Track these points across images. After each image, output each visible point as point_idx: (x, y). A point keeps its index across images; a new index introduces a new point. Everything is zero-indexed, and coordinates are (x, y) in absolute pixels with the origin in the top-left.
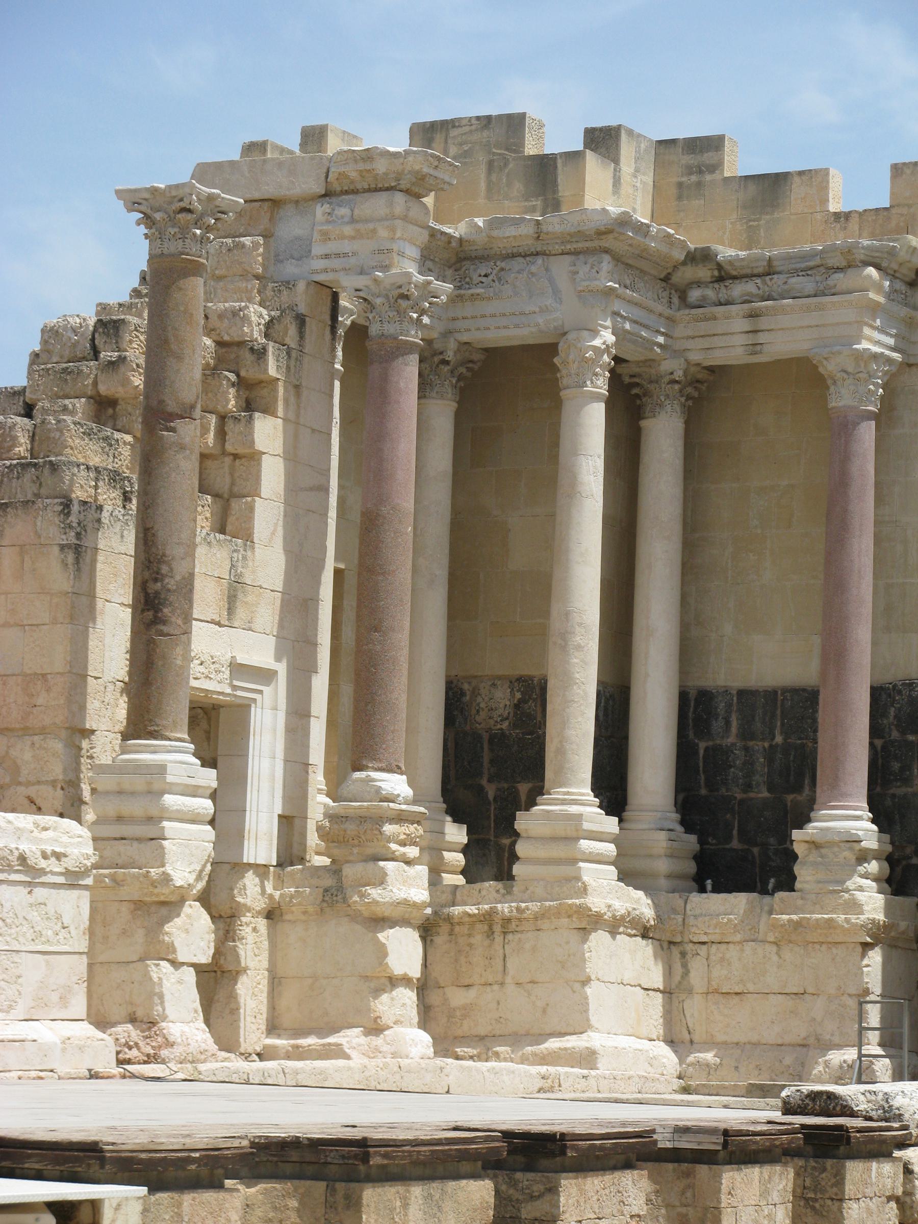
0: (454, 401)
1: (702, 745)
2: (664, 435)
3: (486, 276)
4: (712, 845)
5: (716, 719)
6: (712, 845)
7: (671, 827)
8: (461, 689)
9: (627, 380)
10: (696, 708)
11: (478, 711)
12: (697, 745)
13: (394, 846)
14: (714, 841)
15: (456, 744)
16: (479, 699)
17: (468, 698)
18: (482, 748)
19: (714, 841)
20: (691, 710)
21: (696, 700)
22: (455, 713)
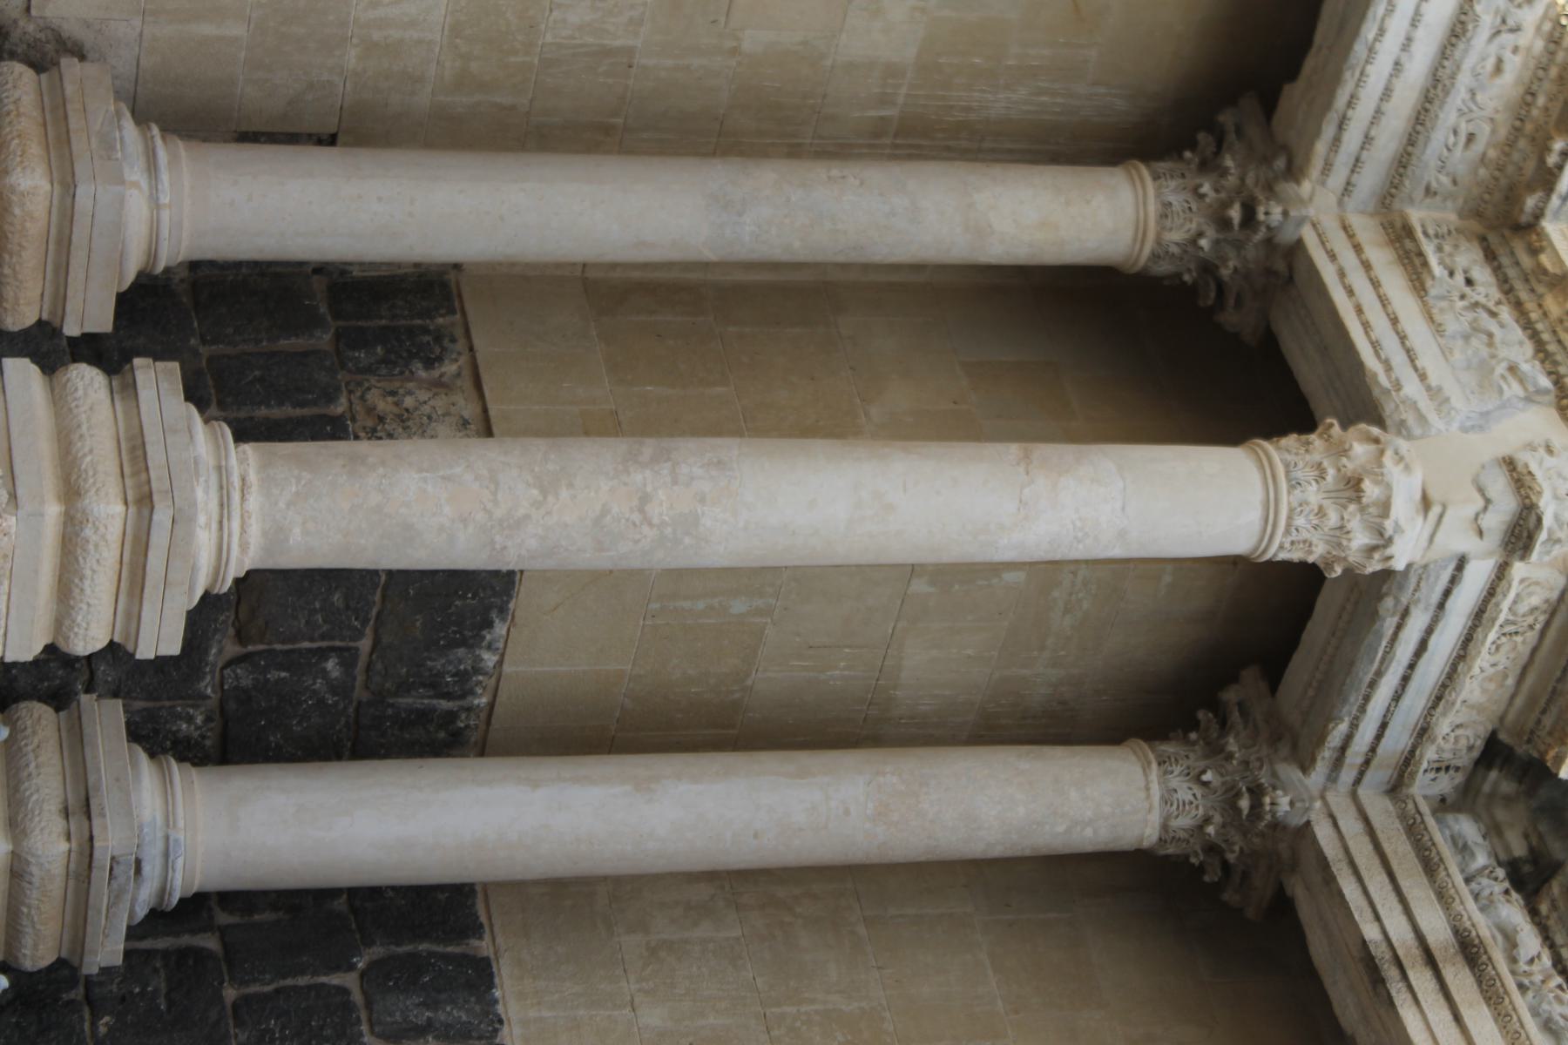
0: (1155, 256)
1: (350, 980)
2: (1115, 798)
3: (1469, 282)
4: (93, 1024)
5: (425, 1005)
6: (93, 1024)
7: (147, 869)
8: (440, 359)
9: (1230, 695)
10: (446, 957)
11: (393, 393)
12: (352, 967)
14: (102, 1030)
15: (305, 354)
16: (423, 395)
17: (423, 374)
18: (302, 405)
19: (102, 1030)
20: (440, 949)
21: (464, 956)
22: (379, 349)
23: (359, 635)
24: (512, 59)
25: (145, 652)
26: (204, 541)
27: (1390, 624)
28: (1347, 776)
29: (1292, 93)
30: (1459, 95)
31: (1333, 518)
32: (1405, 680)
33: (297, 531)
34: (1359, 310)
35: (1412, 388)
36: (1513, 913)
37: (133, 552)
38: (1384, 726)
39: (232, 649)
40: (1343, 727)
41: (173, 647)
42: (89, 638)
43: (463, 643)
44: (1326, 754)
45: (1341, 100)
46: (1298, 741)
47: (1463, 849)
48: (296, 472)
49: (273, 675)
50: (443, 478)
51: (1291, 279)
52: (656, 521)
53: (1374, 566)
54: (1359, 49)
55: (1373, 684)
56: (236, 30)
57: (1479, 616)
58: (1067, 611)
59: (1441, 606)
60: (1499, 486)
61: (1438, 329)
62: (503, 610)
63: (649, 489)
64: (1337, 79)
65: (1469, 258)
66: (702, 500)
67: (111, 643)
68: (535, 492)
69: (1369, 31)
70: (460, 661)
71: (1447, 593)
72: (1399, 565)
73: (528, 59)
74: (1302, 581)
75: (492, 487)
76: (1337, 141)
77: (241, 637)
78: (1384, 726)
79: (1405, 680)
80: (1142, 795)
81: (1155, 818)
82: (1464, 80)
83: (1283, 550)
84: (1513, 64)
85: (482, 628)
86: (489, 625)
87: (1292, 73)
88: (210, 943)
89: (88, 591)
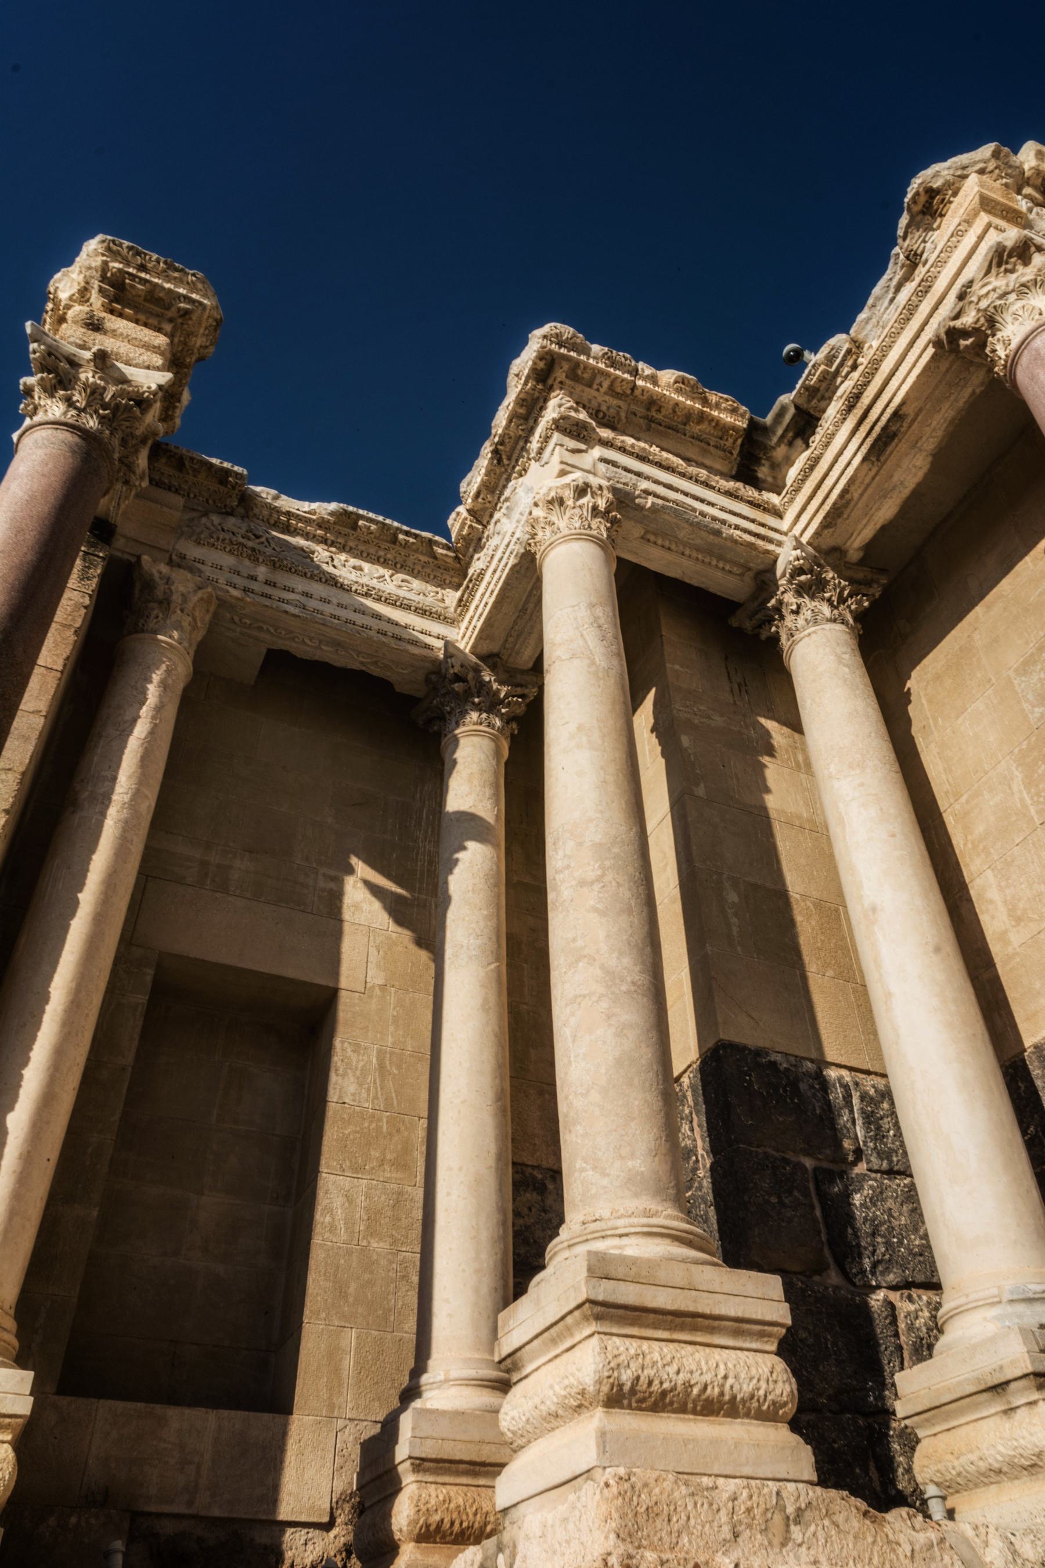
9: (748, 625)
24: (385, 1130)
25: (780, 1313)
26: (638, 1248)
30: (374, 583)
33: (630, 1164)
37: (655, 1326)
43: (794, 1084)
48: (577, 1174)
50: (574, 1041)
52: (599, 872)
56: (351, 1338)
58: (709, 717)
63: (574, 883)
66: (581, 844)
67: (778, 1353)
68: (581, 964)
70: (812, 1087)
73: (385, 1120)
75: (578, 1000)
77: (820, 1269)
80: (813, 636)
84: (353, 561)
85: (778, 1070)
86: (773, 1064)
89: (707, 1377)
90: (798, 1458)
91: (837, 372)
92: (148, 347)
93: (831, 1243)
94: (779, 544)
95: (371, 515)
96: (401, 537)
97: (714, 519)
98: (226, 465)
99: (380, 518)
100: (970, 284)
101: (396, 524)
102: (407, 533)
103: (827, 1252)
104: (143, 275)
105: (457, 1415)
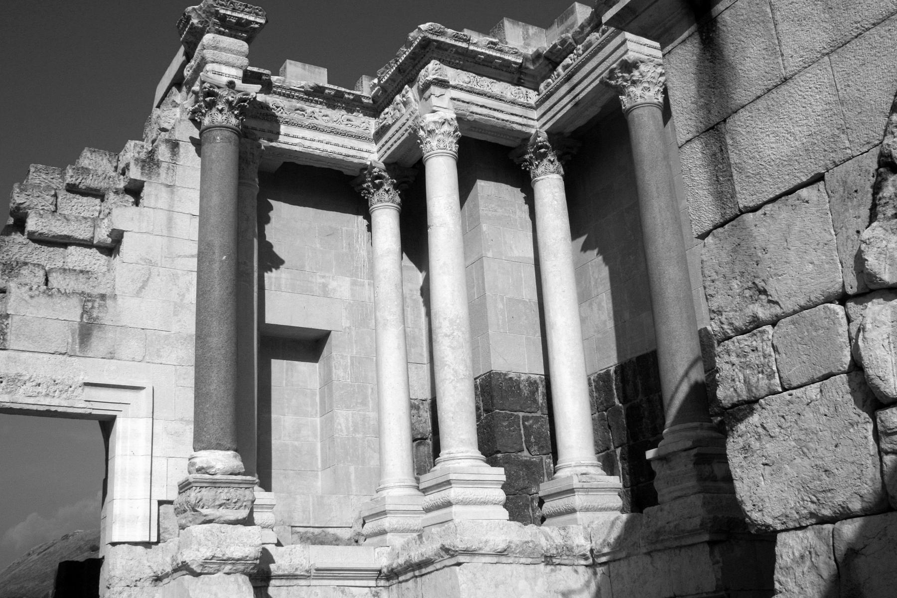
9: (516, 161)
13: (204, 511)
23: (518, 417)
25: (504, 478)
27: (476, 117)
28: (531, 122)
29: (346, 172)
30: (334, 125)
31: (441, 137)
32: (495, 110)
34: (395, 142)
35: (410, 123)
36: (560, 69)
38: (512, 114)
39: (526, 453)
40: (515, 126)
41: (501, 470)
42: (501, 495)
44: (524, 129)
45: (341, 157)
46: (525, 138)
47: (548, 85)
49: (533, 440)
51: (396, 163)
53: (455, 123)
54: (324, 154)
55: (498, 119)
56: (352, 469)
57: (470, 91)
58: (496, 211)
59: (468, 103)
60: (427, 93)
61: (397, 120)
62: (505, 375)
64: (334, 159)
65: (382, 116)
69: (317, 152)
71: (464, 102)
72: (455, 116)
74: (463, 142)
76: (352, 156)
77: (522, 450)
78: (512, 114)
79: (495, 110)
81: (551, 176)
82: (330, 124)
83: (455, 148)
86: (511, 378)
87: (340, 173)
88: (618, 451)
90: (505, 514)
91: (564, 50)
92: (239, 53)
93: (526, 441)
94: (533, 127)
95: (331, 86)
96: (347, 96)
97: (503, 120)
98: (261, 71)
99: (336, 88)
100: (615, 69)
101: (343, 89)
102: (349, 94)
103: (524, 444)
104: (235, 14)
105: (399, 497)
